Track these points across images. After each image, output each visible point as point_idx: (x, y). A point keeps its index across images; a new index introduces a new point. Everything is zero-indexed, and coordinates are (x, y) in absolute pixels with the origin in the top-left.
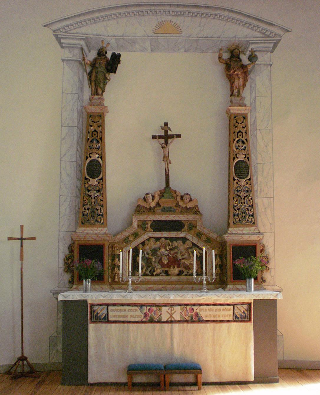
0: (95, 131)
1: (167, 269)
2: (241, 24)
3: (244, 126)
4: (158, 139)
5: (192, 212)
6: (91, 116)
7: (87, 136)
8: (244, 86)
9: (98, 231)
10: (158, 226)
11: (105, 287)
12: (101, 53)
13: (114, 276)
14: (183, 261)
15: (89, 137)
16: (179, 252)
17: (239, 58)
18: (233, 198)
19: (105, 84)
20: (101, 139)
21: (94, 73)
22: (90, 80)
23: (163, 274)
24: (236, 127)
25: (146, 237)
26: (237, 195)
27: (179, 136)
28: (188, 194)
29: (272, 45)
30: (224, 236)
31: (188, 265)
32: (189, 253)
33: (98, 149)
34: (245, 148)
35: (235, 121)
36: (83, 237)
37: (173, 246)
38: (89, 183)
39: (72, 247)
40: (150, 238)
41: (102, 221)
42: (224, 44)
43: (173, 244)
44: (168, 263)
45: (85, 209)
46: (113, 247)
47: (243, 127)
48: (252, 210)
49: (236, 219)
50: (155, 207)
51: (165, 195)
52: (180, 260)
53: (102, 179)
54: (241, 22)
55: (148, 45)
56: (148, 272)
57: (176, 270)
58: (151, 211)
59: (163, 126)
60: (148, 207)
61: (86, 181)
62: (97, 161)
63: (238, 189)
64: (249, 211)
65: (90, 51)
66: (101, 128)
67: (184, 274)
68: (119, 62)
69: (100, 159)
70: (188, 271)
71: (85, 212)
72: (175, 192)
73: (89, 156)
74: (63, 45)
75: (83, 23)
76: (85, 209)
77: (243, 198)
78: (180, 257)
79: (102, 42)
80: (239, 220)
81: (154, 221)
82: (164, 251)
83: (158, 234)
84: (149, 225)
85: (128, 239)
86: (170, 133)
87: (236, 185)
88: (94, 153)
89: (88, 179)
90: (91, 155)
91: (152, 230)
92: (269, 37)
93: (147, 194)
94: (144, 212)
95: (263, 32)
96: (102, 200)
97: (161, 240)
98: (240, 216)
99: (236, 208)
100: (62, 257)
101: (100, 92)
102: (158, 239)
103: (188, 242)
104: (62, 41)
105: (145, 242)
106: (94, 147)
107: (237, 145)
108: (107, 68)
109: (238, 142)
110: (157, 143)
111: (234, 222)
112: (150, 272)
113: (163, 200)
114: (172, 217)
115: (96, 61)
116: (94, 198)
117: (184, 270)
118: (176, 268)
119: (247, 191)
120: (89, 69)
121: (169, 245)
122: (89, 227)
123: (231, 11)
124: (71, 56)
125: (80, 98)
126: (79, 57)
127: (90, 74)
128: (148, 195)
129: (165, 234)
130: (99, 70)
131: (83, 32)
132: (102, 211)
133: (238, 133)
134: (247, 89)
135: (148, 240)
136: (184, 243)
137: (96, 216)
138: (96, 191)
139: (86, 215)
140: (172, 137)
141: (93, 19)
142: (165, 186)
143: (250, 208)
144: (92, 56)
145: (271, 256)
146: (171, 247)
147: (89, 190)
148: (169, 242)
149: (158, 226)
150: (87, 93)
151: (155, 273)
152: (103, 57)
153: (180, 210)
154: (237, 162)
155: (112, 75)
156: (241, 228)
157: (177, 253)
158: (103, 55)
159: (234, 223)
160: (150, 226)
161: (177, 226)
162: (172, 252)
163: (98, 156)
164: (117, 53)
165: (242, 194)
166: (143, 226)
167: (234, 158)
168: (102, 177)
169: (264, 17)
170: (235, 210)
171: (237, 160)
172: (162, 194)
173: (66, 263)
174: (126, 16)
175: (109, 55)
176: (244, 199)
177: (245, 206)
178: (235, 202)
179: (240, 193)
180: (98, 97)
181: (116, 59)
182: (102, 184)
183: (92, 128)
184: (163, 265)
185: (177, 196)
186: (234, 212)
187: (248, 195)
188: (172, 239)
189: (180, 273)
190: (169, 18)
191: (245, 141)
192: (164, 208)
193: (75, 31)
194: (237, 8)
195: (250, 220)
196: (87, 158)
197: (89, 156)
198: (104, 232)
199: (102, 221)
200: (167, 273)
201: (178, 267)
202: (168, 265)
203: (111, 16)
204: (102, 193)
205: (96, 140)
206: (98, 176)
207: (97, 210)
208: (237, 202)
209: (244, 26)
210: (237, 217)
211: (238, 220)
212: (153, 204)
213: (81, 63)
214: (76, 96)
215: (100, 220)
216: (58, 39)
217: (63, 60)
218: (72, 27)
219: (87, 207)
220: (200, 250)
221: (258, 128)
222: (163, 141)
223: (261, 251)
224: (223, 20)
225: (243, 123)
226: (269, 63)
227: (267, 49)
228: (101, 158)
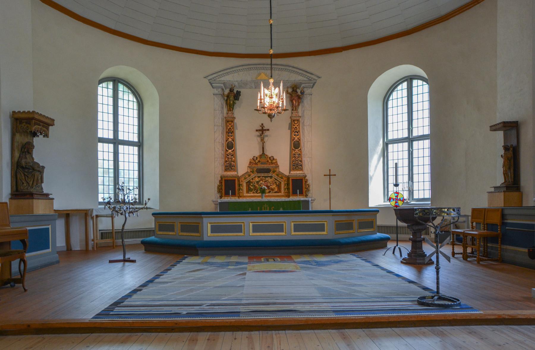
2: (298, 74)
6: (228, 121)
7: (226, 130)
8: (299, 105)
9: (233, 174)
11: (236, 198)
12: (231, 90)
13: (239, 193)
14: (271, 187)
17: (296, 91)
19: (234, 106)
20: (233, 132)
21: (228, 101)
22: (227, 104)
27: (268, 130)
28: (273, 157)
29: (312, 85)
34: (298, 135)
38: (228, 152)
40: (256, 176)
42: (289, 85)
46: (239, 181)
54: (298, 73)
55: (253, 86)
56: (255, 192)
59: (261, 125)
65: (226, 89)
67: (271, 192)
68: (240, 95)
69: (232, 141)
72: (267, 155)
74: (214, 87)
75: (222, 75)
76: (227, 164)
77: (297, 158)
79: (232, 85)
80: (295, 168)
83: (259, 175)
84: (255, 171)
86: (264, 128)
87: (294, 152)
92: (311, 80)
93: (254, 157)
95: (308, 78)
99: (294, 162)
100: (216, 186)
101: (231, 109)
102: (259, 177)
103: (273, 178)
104: (213, 85)
106: (230, 135)
108: (234, 97)
109: (295, 132)
110: (258, 133)
112: (256, 192)
113: (261, 159)
115: (229, 94)
117: (271, 190)
119: (299, 155)
120: (226, 98)
123: (293, 67)
124: (217, 92)
125: (222, 113)
126: (221, 92)
127: (227, 100)
129: (263, 175)
130: (231, 99)
131: (223, 80)
133: (295, 128)
134: (300, 107)
135: (255, 177)
136: (271, 179)
140: (265, 130)
141: (227, 73)
143: (300, 162)
144: (227, 92)
145: (310, 184)
147: (228, 155)
150: (225, 110)
151: (258, 192)
152: (232, 93)
155: (236, 101)
156: (296, 172)
157: (268, 183)
158: (233, 91)
159: (293, 169)
161: (268, 171)
162: (266, 183)
164: (239, 91)
167: (293, 140)
169: (308, 70)
172: (261, 156)
173: (218, 188)
174: (243, 71)
175: (235, 92)
180: (231, 112)
181: (239, 93)
185: (268, 157)
188: (266, 177)
190: (263, 71)
192: (262, 163)
193: (219, 79)
194: (296, 66)
195: (300, 168)
196: (227, 141)
198: (235, 174)
203: (235, 71)
206: (232, 149)
207: (232, 164)
209: (299, 75)
210: (294, 167)
212: (257, 161)
213: (222, 95)
214: (220, 112)
216: (211, 84)
217: (214, 94)
218: (217, 77)
219: (227, 163)
221: (305, 125)
222: (261, 132)
223: (306, 182)
224: (289, 72)
226: (310, 93)
227: (310, 87)
228: (233, 141)
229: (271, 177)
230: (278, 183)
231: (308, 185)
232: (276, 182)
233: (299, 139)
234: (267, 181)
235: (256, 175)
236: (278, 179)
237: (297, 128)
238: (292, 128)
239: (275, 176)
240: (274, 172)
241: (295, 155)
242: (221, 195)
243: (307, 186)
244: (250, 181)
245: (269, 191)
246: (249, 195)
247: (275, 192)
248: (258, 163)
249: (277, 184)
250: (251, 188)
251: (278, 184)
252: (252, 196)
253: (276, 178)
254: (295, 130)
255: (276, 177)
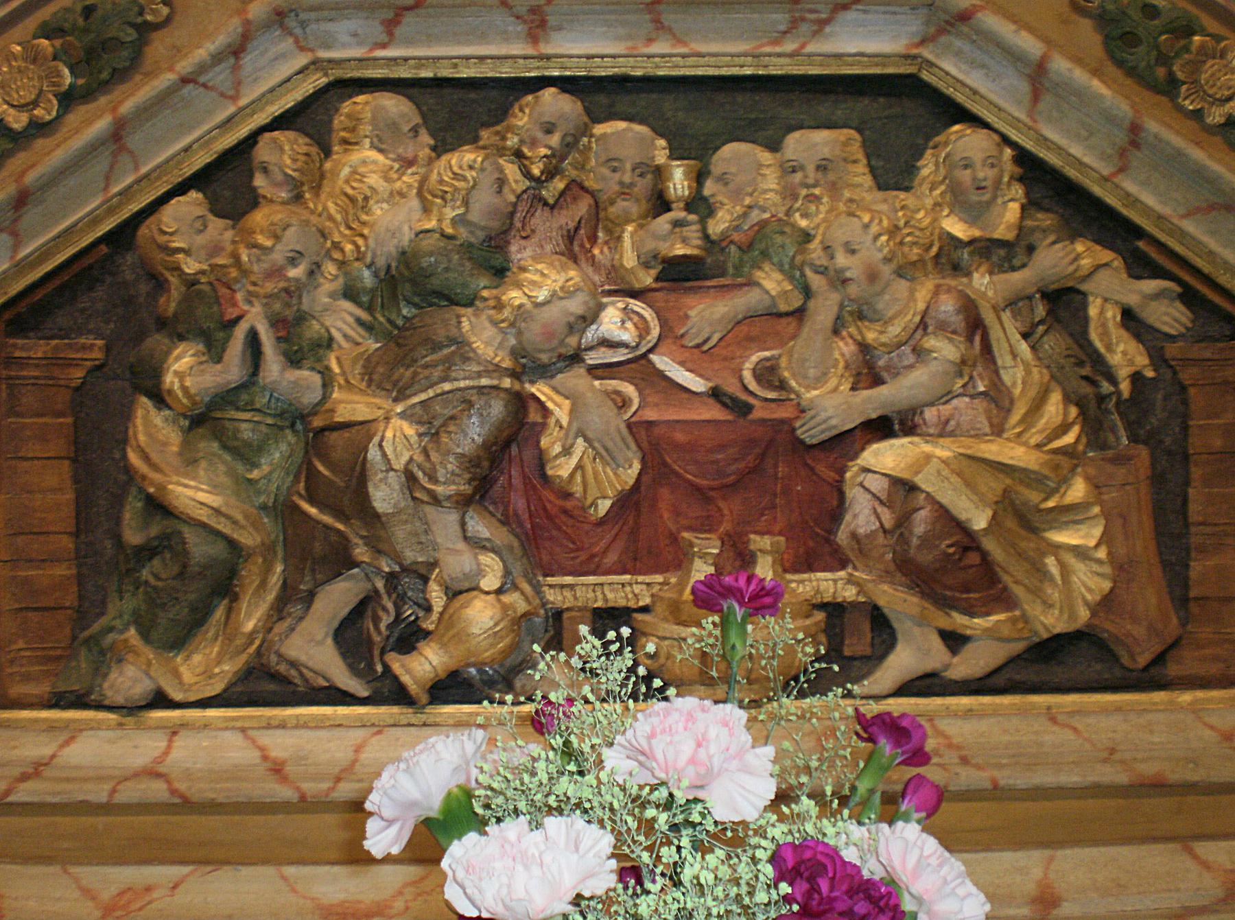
16: (824, 309)
31: (961, 527)
32: (974, 325)
37: (718, 225)
43: (709, 188)
44: (628, 501)
70: (959, 621)
82: (576, 306)
97: (522, 119)
105: (263, 151)
121: (661, 204)
146: (693, 232)
148: (660, 152)
220: (1151, 285)
239: (1037, 75)
244: (122, 236)
249: (1100, 366)
250: (158, 507)
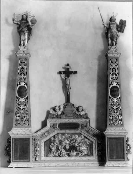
0: (23, 68)
1: (69, 152)
3: (116, 65)
4: (62, 73)
5: (84, 117)
10: (63, 126)
15: (18, 72)
18: (109, 110)
20: (26, 73)
23: (66, 156)
24: (111, 65)
25: (56, 133)
26: (112, 107)
28: (81, 106)
30: (104, 132)
33: (25, 79)
34: (117, 78)
35: (111, 61)
36: (16, 134)
37: (73, 138)
38: (19, 100)
39: (10, 140)
40: (58, 133)
41: (28, 124)
44: (69, 149)
45: (17, 116)
47: (116, 65)
48: (121, 117)
49: (111, 122)
50: (61, 115)
51: (66, 107)
52: (77, 147)
53: (27, 98)
56: (57, 155)
57: (75, 153)
58: (58, 117)
60: (57, 115)
61: (17, 100)
62: (24, 87)
63: (113, 104)
64: (119, 118)
66: (26, 66)
67: (79, 155)
69: (26, 86)
71: (17, 118)
72: (73, 105)
73: (19, 84)
76: (17, 116)
78: (76, 145)
80: (113, 123)
81: (60, 123)
83: (63, 131)
84: (57, 126)
85: (44, 134)
86: (70, 70)
88: (22, 82)
89: (18, 98)
90: (20, 83)
91: (59, 129)
94: (54, 117)
96: (28, 111)
98: (113, 121)
102: (63, 134)
103: (82, 136)
106: (22, 78)
107: (112, 76)
109: (112, 75)
111: (110, 123)
114: (72, 121)
116: (23, 110)
117: (79, 152)
118: (74, 152)
119: (118, 105)
122: (20, 127)
128: (56, 107)
129: (68, 131)
132: (28, 118)
133: (112, 69)
137: (24, 121)
138: (24, 105)
139: (18, 120)
140: (72, 72)
142: (65, 102)
147: (19, 105)
149: (63, 126)
151: (61, 155)
153: (77, 116)
154: (112, 87)
160: (58, 127)
161: (74, 126)
162: (72, 142)
163: (24, 83)
165: (115, 107)
166: (53, 127)
167: (110, 85)
168: (28, 97)
170: (110, 117)
171: (111, 86)
176: (116, 110)
177: (117, 114)
178: (110, 112)
179: (114, 106)
182: (27, 101)
183: (21, 66)
184: (66, 150)
185: (74, 107)
186: (110, 118)
187: (118, 108)
189: (77, 154)
191: (117, 74)
197: (19, 84)
199: (28, 124)
200: (69, 155)
201: (76, 151)
202: (69, 150)
204: (27, 106)
205: (23, 74)
206: (25, 96)
208: (111, 112)
210: (111, 121)
211: (112, 123)
212: (60, 113)
215: (26, 123)
219: (18, 115)
223: (127, 141)
225: (116, 63)
229: (80, 134)
230: (88, 142)
231: (129, 145)
232: (86, 141)
233: (118, 83)
234: (74, 139)
235: (59, 132)
236: (88, 138)
237: (115, 69)
238: (109, 69)
240: (82, 128)
241: (112, 105)
242: (8, 160)
243: (128, 147)
245: (77, 153)
246: (48, 159)
247: (85, 155)
248: (61, 116)
251: (88, 143)
252: (52, 161)
253: (86, 136)
254: (112, 72)
255: (86, 134)
